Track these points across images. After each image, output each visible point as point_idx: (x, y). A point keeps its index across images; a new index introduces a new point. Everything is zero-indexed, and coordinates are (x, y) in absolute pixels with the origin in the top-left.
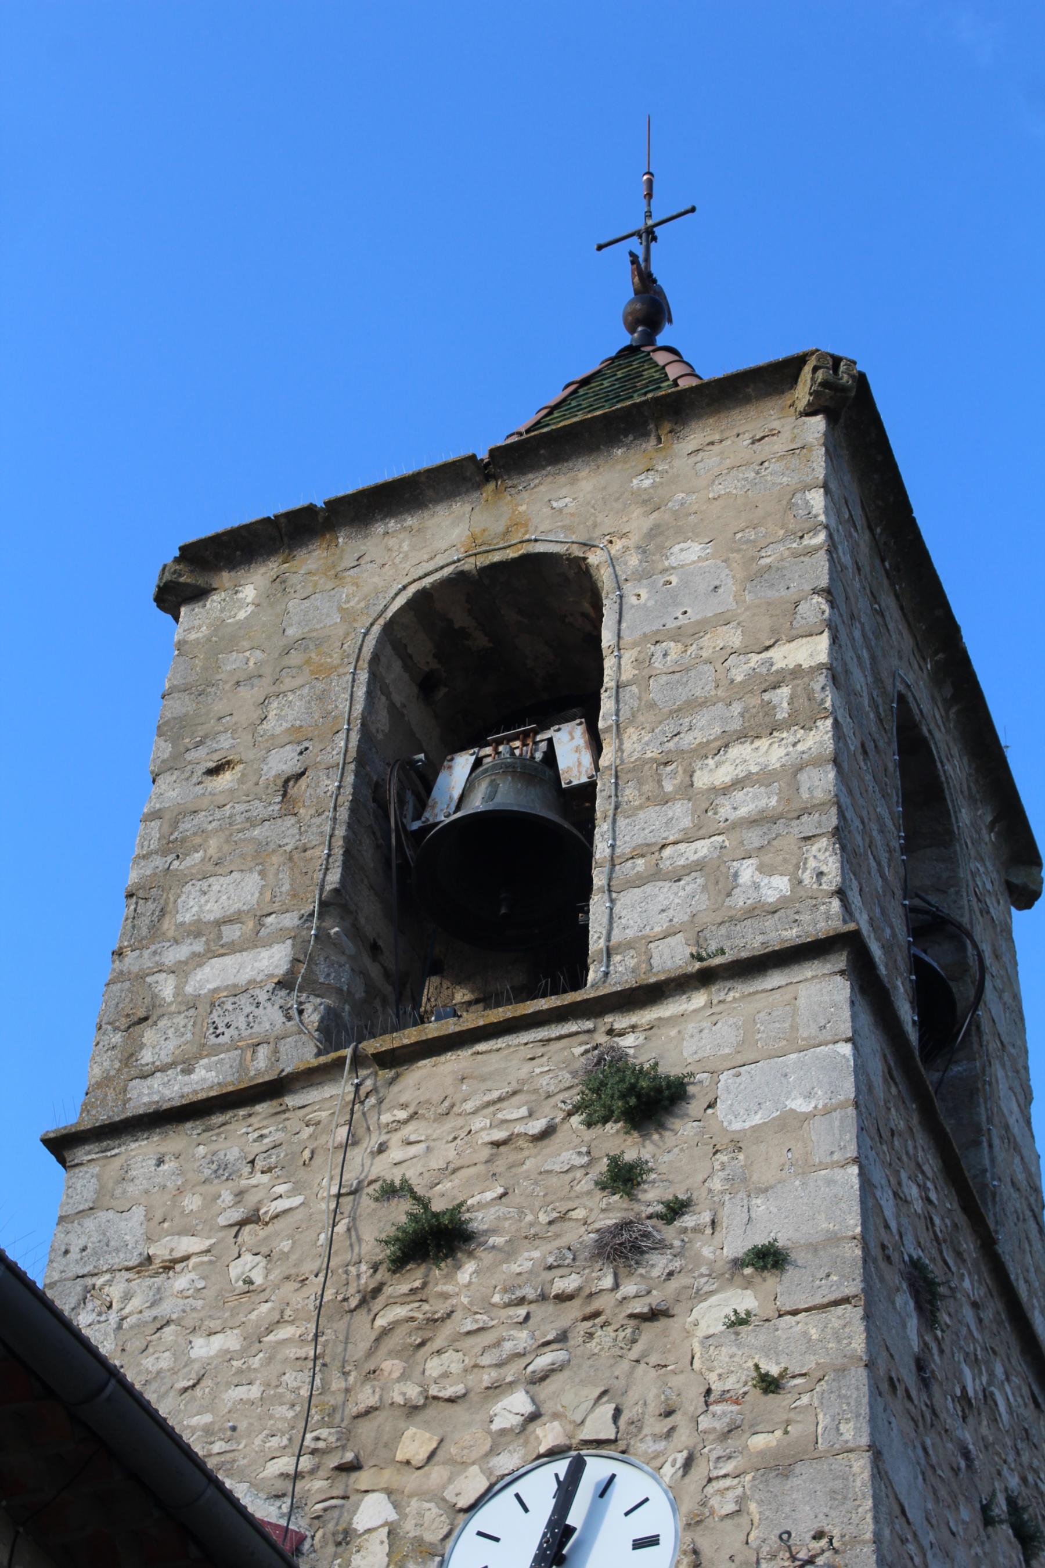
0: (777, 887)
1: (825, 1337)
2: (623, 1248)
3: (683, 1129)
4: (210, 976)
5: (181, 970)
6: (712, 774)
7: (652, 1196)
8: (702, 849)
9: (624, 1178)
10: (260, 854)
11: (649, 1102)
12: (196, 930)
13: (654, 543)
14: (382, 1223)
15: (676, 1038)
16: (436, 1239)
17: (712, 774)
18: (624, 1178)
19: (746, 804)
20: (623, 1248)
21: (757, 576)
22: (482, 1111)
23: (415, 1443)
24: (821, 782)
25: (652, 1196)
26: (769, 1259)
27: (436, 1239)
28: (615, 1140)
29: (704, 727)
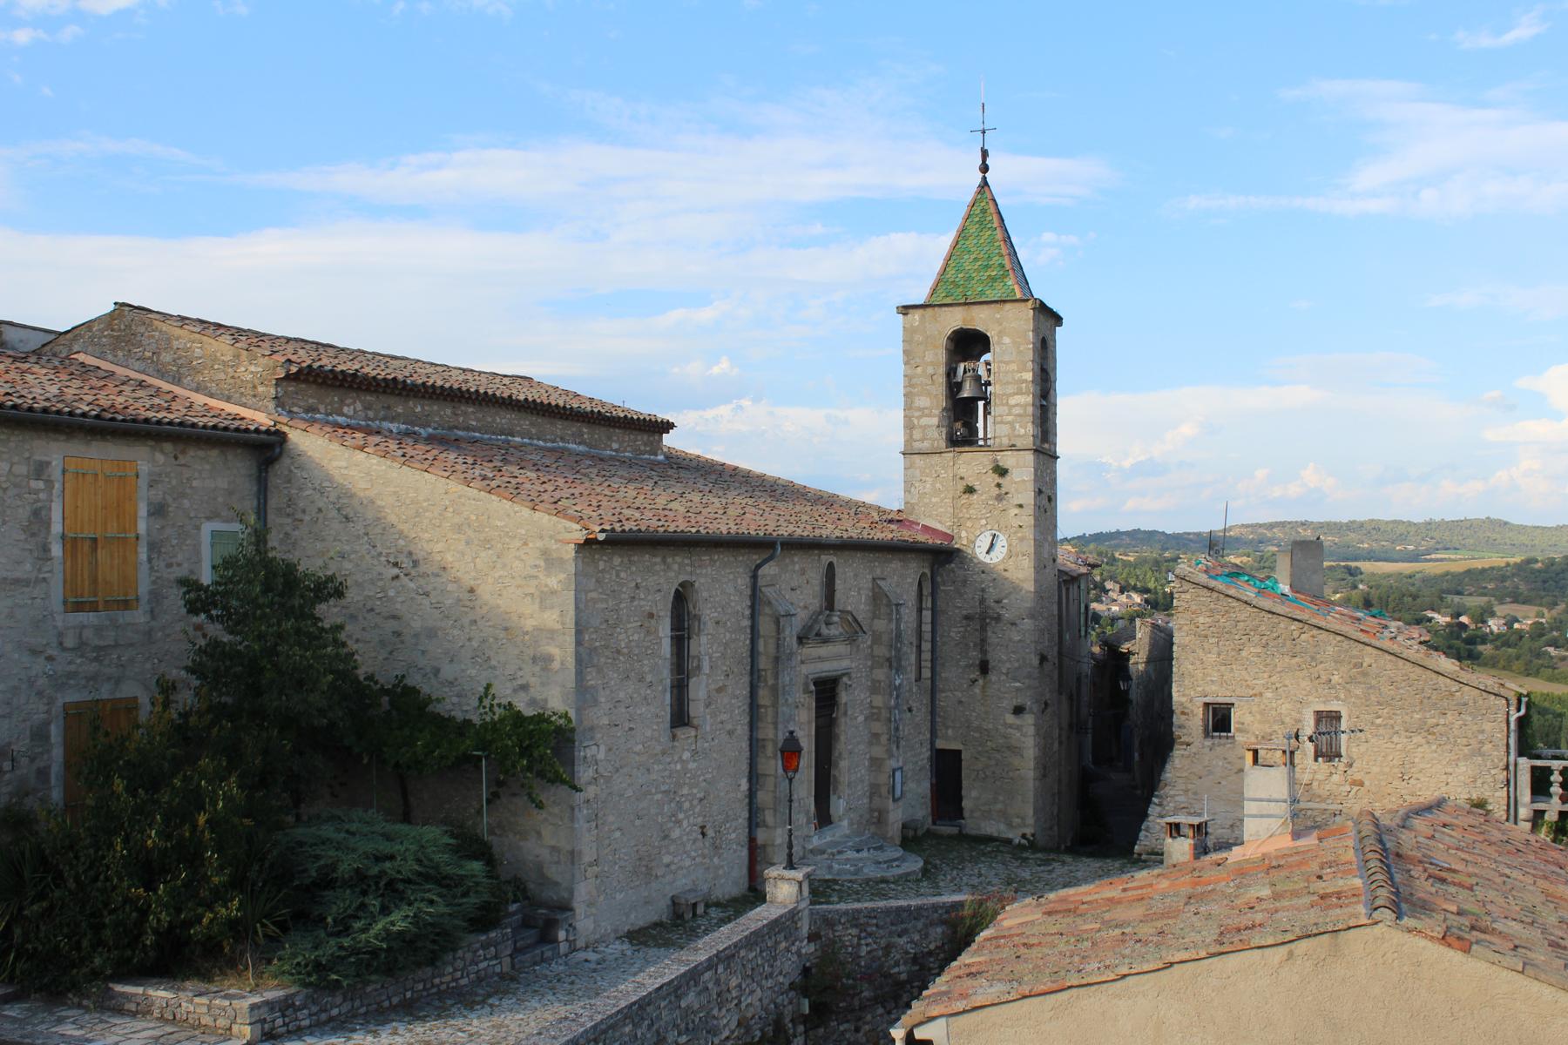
0: (1022, 431)
1: (1027, 518)
2: (999, 498)
3: (1008, 478)
4: (924, 421)
5: (919, 418)
6: (1012, 401)
7: (1004, 490)
8: (1010, 418)
9: (999, 485)
10: (929, 394)
11: (1002, 472)
12: (919, 409)
13: (1001, 334)
14: (961, 486)
15: (1007, 460)
16: (970, 490)
17: (1012, 401)
18: (999, 485)
19: (1017, 411)
20: (999, 498)
21: (1020, 352)
22: (972, 465)
23: (969, 524)
24: (1030, 410)
25: (1004, 490)
26: (1021, 506)
27: (970, 490)
28: (998, 479)
29: (1010, 389)
